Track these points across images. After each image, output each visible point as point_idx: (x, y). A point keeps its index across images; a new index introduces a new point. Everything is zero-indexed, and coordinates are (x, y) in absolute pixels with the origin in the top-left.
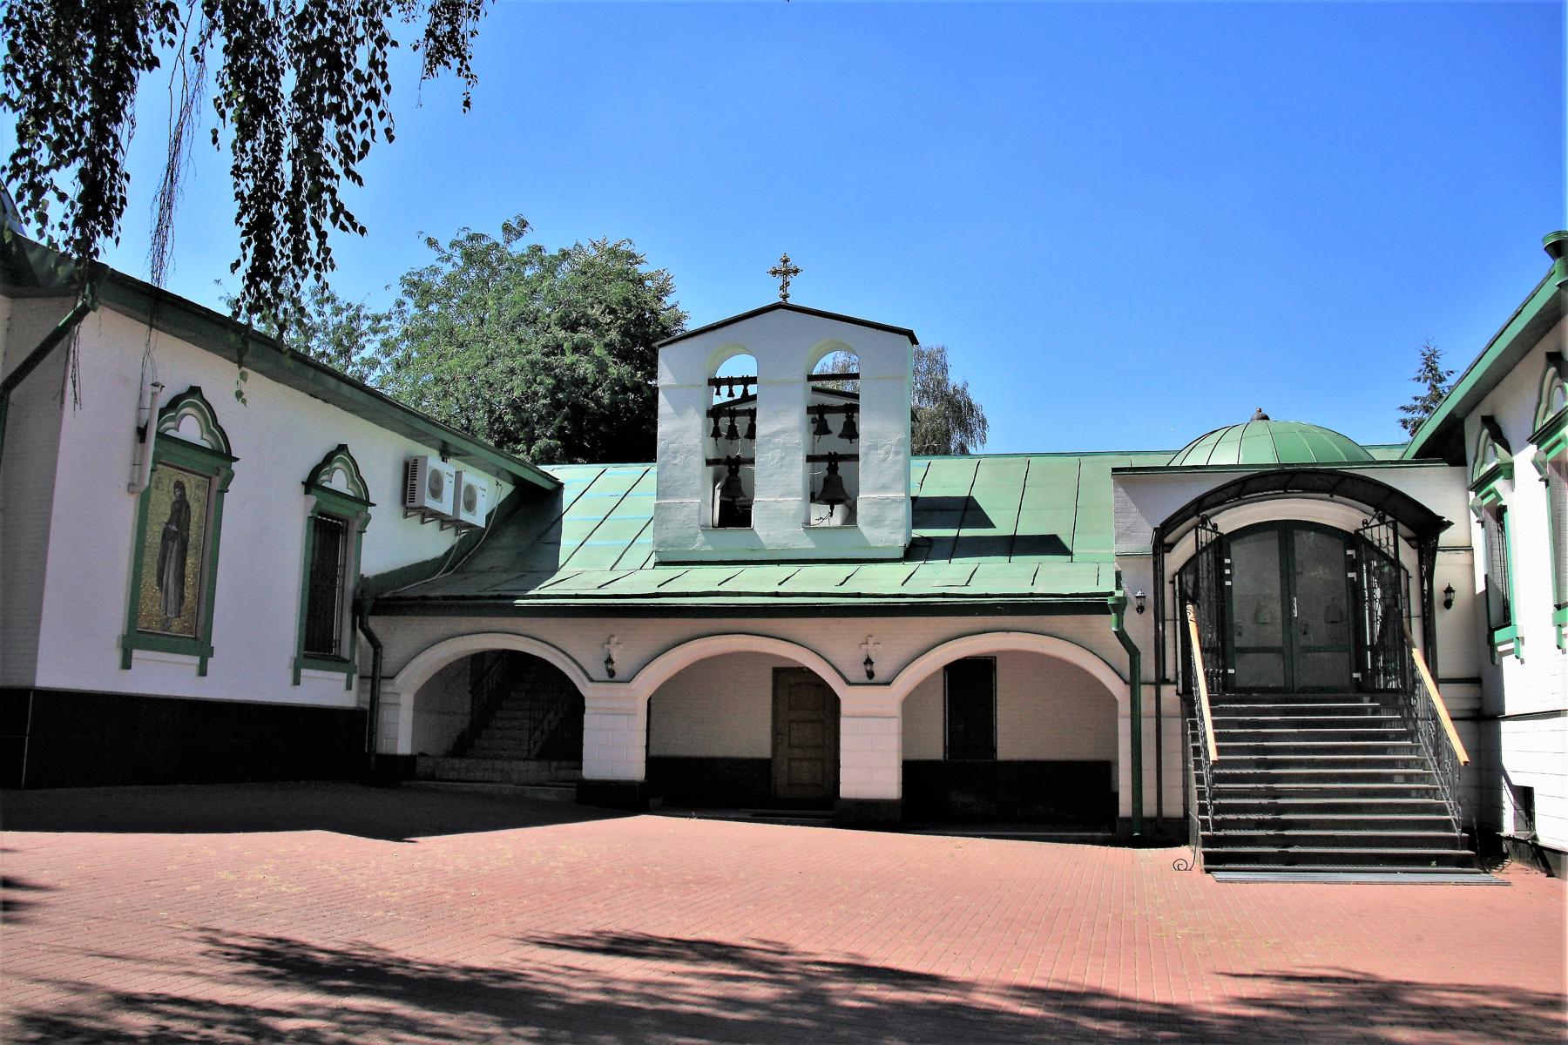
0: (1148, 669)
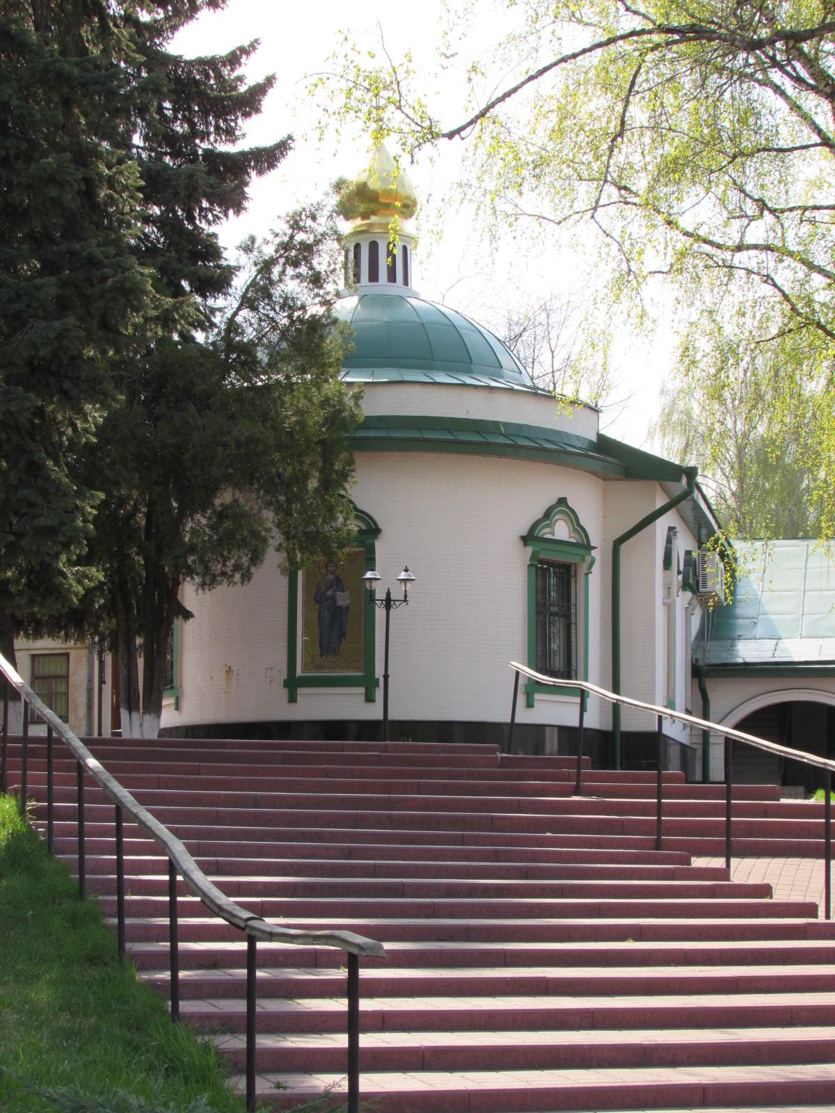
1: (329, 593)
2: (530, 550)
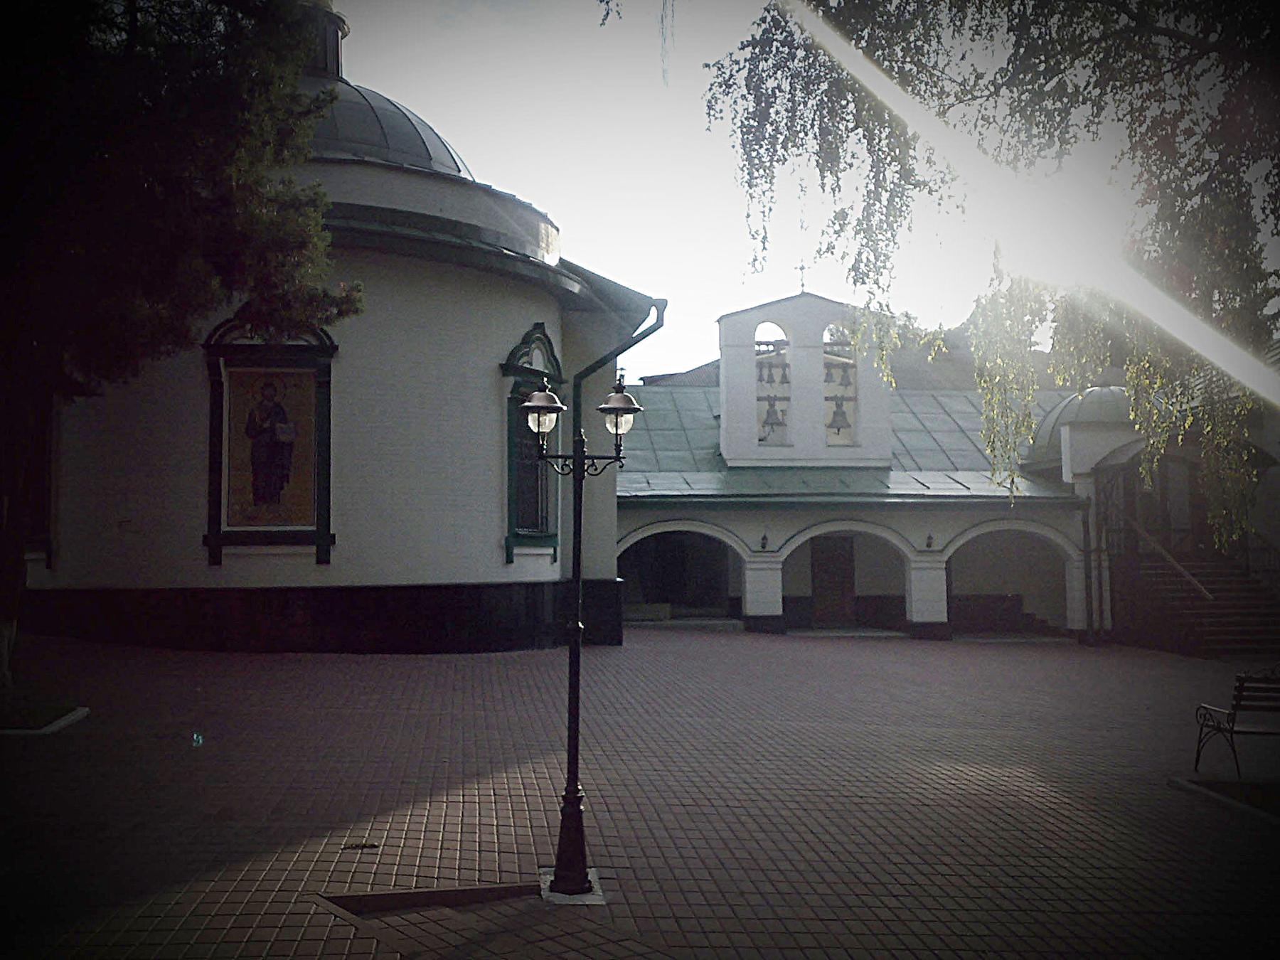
0: (1093, 545)
1: (266, 425)
2: (511, 380)
